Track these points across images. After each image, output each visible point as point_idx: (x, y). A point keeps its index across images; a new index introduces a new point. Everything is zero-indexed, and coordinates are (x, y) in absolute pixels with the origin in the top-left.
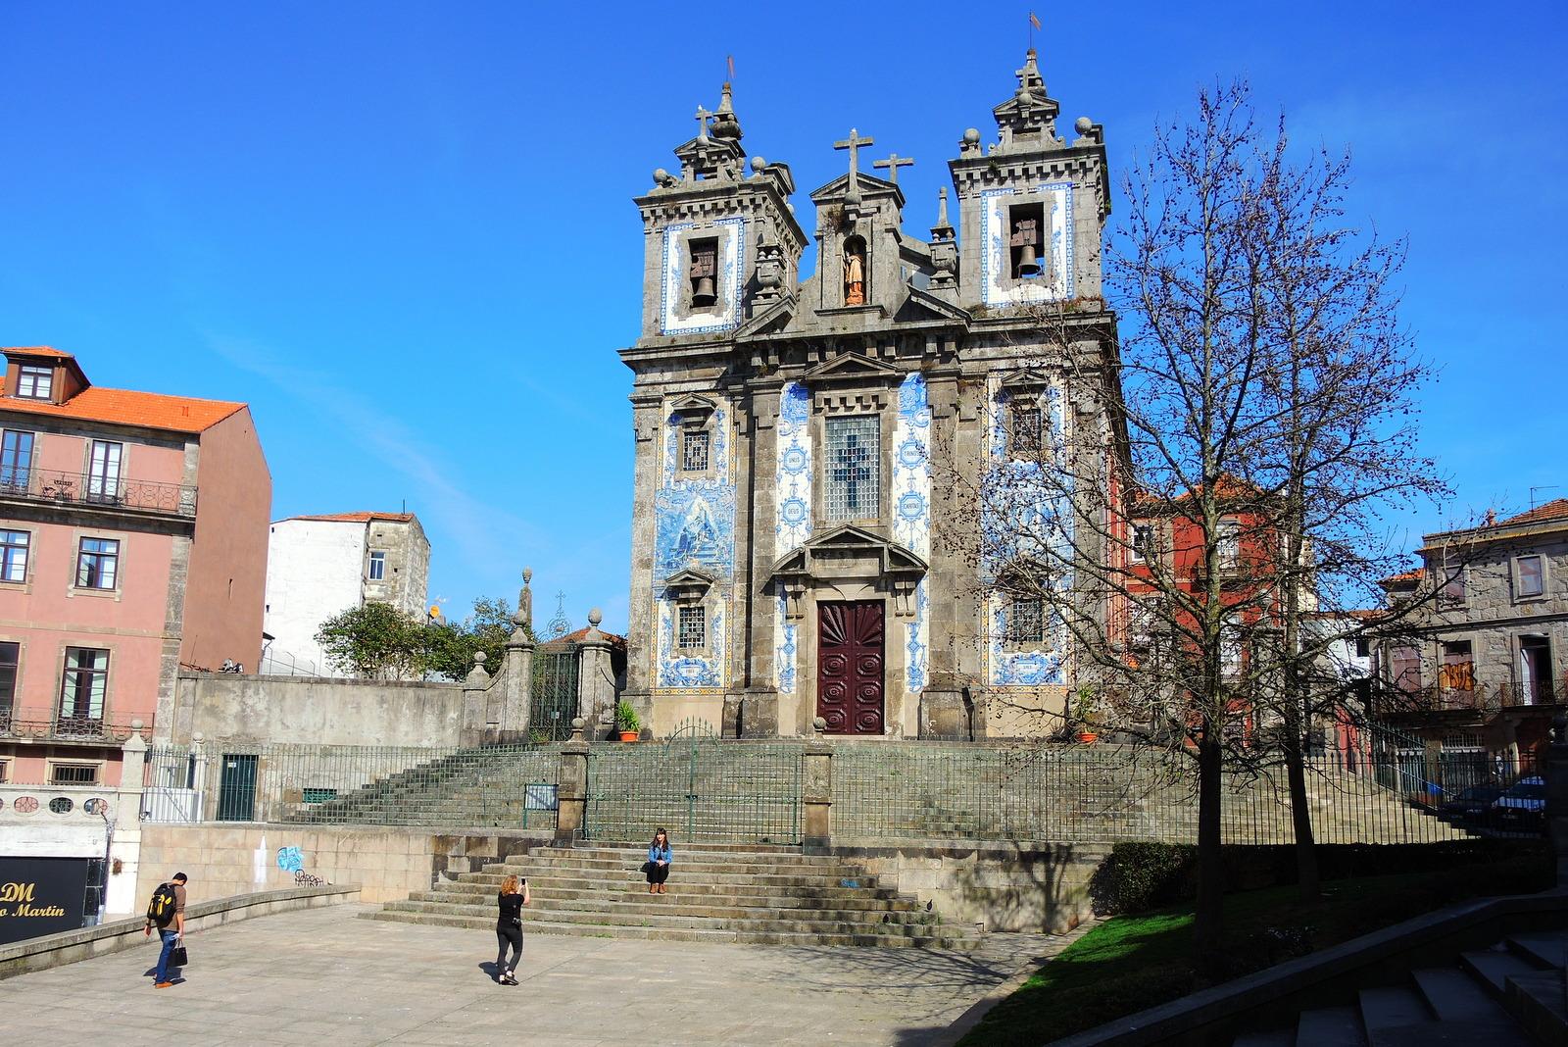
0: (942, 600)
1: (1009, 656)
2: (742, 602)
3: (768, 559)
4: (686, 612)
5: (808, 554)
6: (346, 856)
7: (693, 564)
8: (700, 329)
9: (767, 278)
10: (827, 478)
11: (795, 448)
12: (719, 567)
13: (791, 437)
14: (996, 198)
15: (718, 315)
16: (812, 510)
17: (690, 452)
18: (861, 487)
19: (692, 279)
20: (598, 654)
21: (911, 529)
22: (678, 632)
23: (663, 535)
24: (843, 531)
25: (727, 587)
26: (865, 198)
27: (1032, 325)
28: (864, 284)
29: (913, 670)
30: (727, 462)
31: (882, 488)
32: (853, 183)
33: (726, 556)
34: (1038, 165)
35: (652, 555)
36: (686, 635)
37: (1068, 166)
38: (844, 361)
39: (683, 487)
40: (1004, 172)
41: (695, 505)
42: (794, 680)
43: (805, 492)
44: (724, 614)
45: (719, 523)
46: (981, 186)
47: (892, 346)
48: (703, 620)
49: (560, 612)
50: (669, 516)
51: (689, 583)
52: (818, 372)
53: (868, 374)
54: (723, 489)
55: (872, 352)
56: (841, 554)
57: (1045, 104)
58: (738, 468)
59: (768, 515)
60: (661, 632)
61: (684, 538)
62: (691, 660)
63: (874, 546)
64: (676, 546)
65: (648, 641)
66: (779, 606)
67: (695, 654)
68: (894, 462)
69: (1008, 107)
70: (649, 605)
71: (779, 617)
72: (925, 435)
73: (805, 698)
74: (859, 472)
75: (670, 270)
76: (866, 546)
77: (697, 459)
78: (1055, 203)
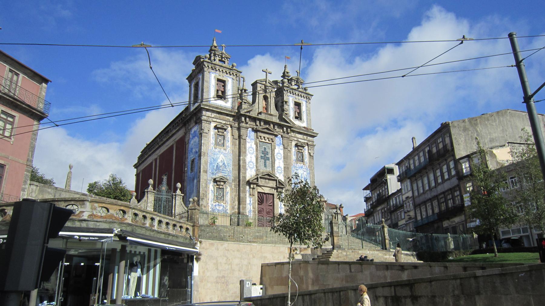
3: (245, 177)
12: (228, 177)
13: (250, 144)
15: (226, 103)
17: (218, 140)
20: (181, 198)
22: (216, 195)
23: (211, 164)
25: (230, 183)
26: (270, 87)
32: (267, 81)
33: (230, 174)
39: (217, 150)
40: (294, 93)
42: (252, 213)
43: (254, 160)
51: (222, 180)
52: (259, 128)
55: (272, 125)
56: (266, 179)
59: (244, 164)
60: (210, 194)
61: (217, 166)
62: (219, 204)
64: (215, 168)
65: (206, 197)
68: (276, 157)
70: (207, 185)
71: (248, 194)
72: (282, 152)
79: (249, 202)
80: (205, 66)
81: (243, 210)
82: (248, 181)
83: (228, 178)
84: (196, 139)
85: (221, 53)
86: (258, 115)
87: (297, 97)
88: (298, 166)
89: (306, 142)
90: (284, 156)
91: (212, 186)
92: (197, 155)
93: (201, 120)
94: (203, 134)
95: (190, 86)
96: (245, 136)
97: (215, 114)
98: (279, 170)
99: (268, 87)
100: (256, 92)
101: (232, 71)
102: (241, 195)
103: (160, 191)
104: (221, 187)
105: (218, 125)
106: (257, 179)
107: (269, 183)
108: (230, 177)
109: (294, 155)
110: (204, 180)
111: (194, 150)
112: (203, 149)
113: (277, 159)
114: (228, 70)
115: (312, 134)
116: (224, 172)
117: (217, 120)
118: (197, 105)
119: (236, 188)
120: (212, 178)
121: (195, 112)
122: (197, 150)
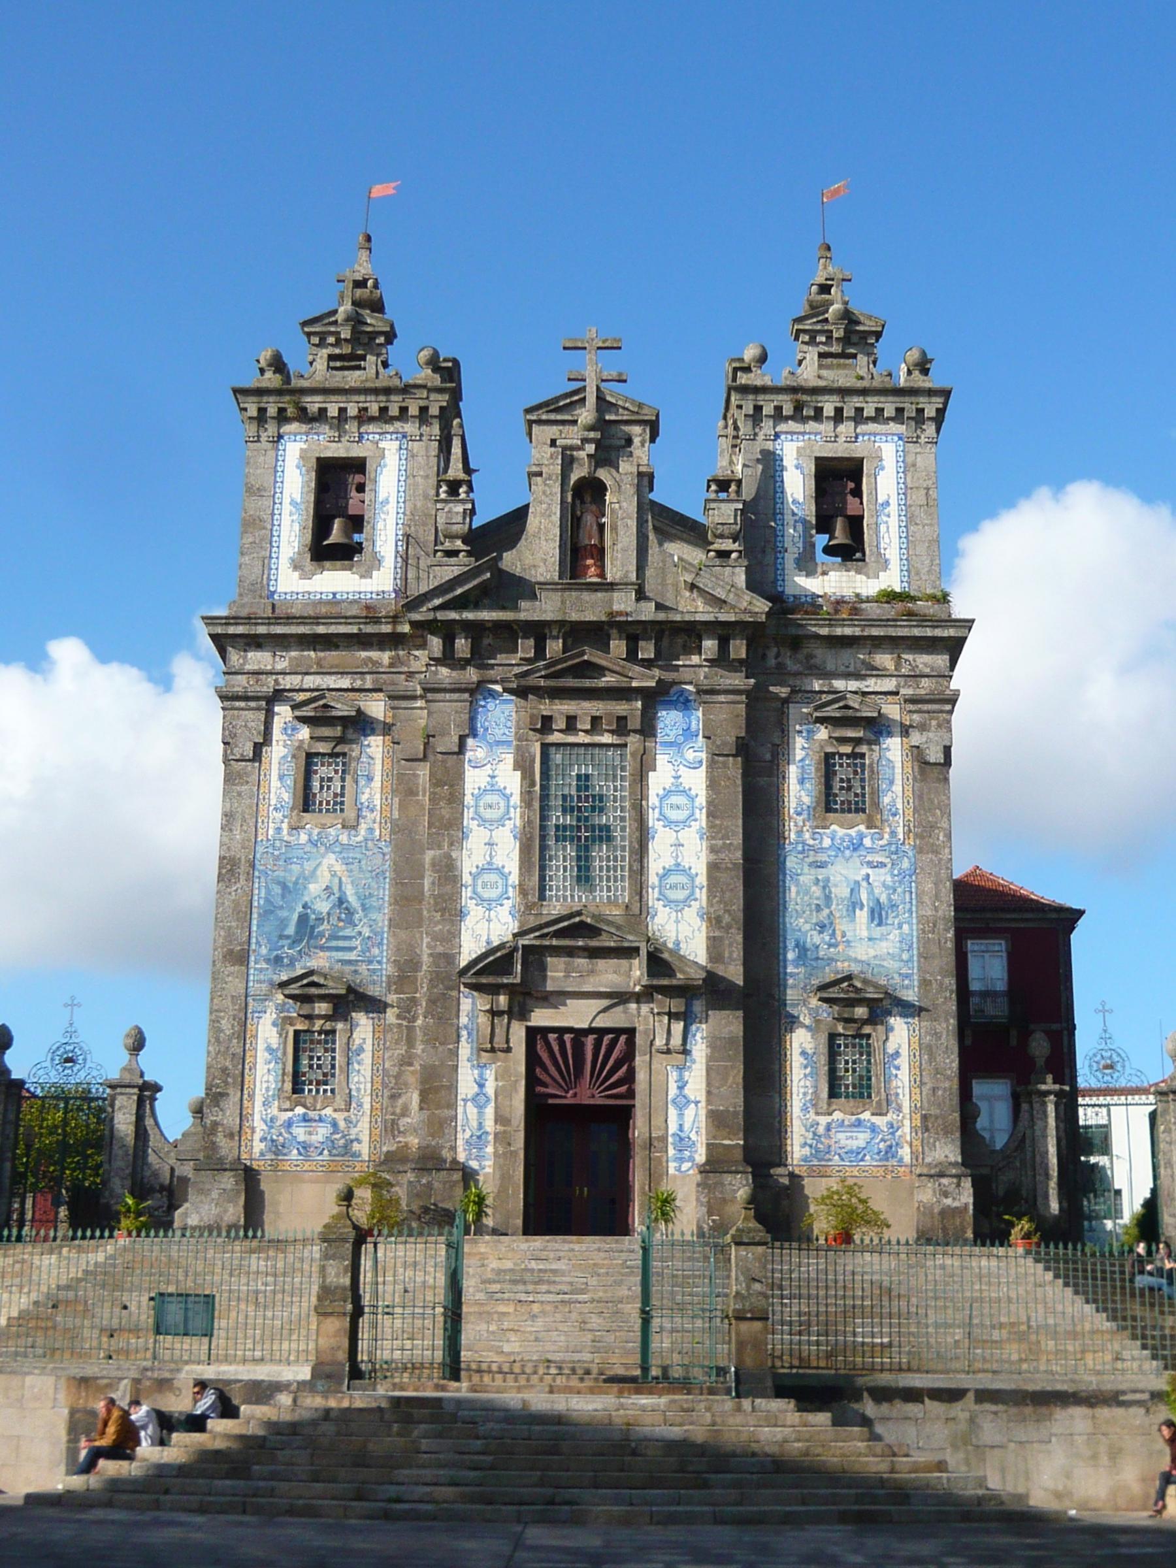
0: (725, 1033)
1: (823, 1120)
2: (400, 1025)
3: (450, 958)
7: (319, 961)
8: (334, 594)
9: (455, 527)
10: (543, 838)
11: (493, 788)
12: (363, 968)
13: (488, 770)
14: (795, 445)
15: (367, 575)
16: (520, 885)
18: (600, 853)
21: (677, 922)
22: (289, 1068)
24: (577, 919)
27: (857, 632)
28: (599, 553)
29: (683, 1142)
30: (377, 802)
34: (858, 405)
36: (304, 1074)
37: (900, 411)
39: (303, 838)
41: (324, 867)
42: (490, 1149)
43: (509, 856)
44: (369, 1042)
45: (363, 899)
47: (648, 639)
48: (334, 1050)
49: (71, 1032)
50: (279, 883)
51: (314, 991)
54: (370, 844)
56: (570, 952)
61: (303, 919)
62: (312, 1114)
63: (626, 944)
64: (291, 930)
68: (652, 818)
72: (697, 781)
73: (505, 1177)
74: (593, 831)
75: (286, 501)
77: (326, 796)
78: (881, 460)
79: (476, 1089)
81: (433, 1136)
87: (826, 427)
88: (827, 842)
89: (889, 685)
90: (710, 803)
91: (274, 1024)
96: (456, 739)
101: (393, 398)
104: (318, 1024)
108: (376, 966)
109: (801, 781)
110: (228, 1002)
113: (658, 825)
114: (373, 398)
115: (929, 632)
116: (346, 944)
117: (308, 678)
119: (414, 1019)
120: (271, 983)
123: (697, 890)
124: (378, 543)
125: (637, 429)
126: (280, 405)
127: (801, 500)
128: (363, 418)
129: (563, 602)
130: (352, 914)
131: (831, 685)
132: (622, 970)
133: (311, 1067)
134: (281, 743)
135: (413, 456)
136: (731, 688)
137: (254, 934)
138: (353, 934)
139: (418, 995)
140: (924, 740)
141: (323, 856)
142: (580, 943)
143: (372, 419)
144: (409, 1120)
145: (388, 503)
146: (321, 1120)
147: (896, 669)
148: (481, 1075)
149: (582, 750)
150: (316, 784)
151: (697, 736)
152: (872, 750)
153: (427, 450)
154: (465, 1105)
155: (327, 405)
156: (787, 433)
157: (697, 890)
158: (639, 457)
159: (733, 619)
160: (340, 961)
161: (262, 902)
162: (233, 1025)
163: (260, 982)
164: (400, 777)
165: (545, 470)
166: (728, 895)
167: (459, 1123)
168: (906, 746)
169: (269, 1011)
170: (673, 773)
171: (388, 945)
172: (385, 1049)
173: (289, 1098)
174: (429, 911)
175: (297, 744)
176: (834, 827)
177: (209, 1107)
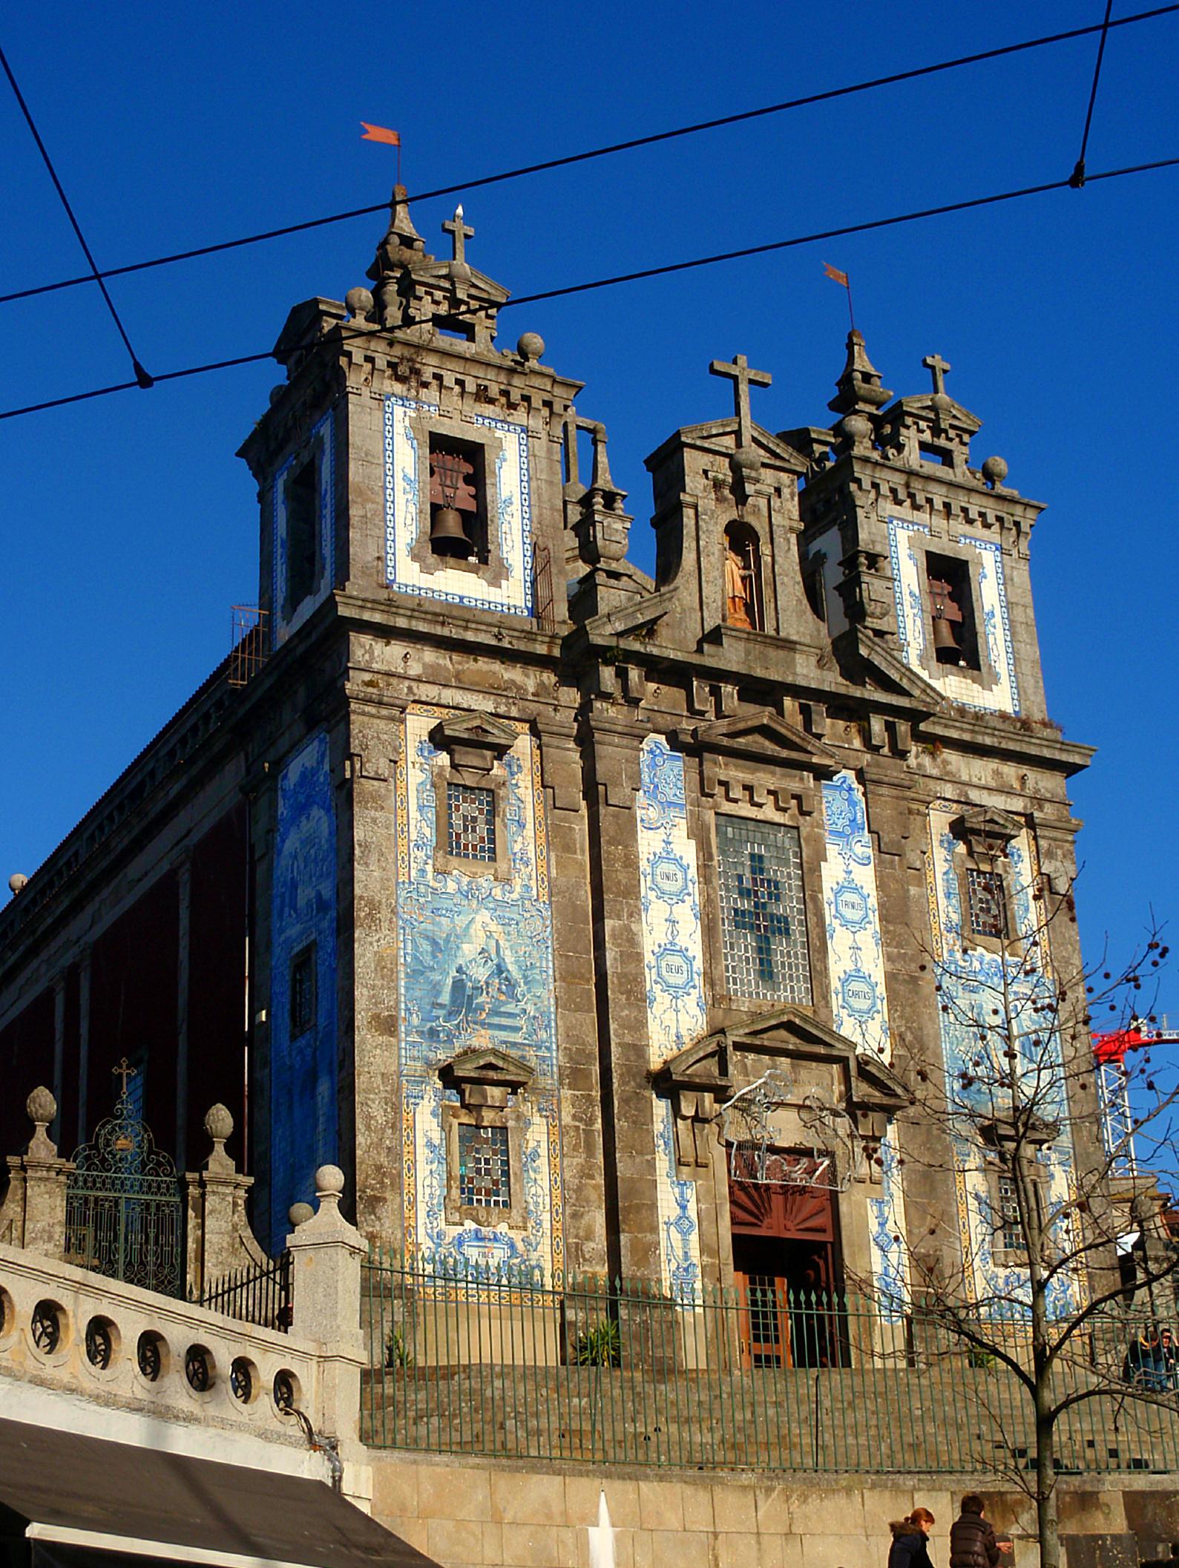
2: (577, 1128)
3: (639, 1051)
4: (471, 1135)
5: (730, 1049)
6: (779, 1541)
7: (482, 1039)
8: (461, 598)
11: (667, 856)
12: (530, 1053)
15: (495, 582)
18: (779, 946)
19: (433, 505)
20: (235, 1204)
22: (457, 1171)
23: (416, 973)
24: (785, 1018)
26: (764, 465)
30: (532, 855)
31: (815, 956)
34: (963, 504)
35: (397, 1007)
38: (755, 723)
39: (452, 887)
40: (920, 499)
41: (477, 926)
44: (544, 1145)
45: (526, 969)
46: (888, 507)
48: (506, 1152)
50: (427, 938)
51: (492, 1075)
53: (795, 755)
57: (964, 419)
58: (554, 872)
59: (631, 968)
60: (423, 1170)
61: (458, 986)
62: (485, 1231)
63: (835, 1053)
64: (445, 998)
65: (397, 1184)
66: (661, 1142)
67: (494, 1220)
68: (828, 913)
69: (919, 405)
70: (397, 1109)
71: (663, 1163)
72: (866, 877)
75: (399, 475)
76: (823, 1052)
79: (678, 1211)
80: (350, 363)
82: (664, 1074)
83: (533, 1063)
84: (319, 822)
85: (444, 271)
86: (700, 650)
88: (976, 965)
89: (1018, 805)
91: (434, 1114)
92: (325, 924)
93: (345, 701)
94: (363, 788)
95: (261, 497)
96: (628, 790)
97: (429, 655)
98: (856, 994)
99: (751, 467)
100: (679, 506)
101: (517, 381)
102: (622, 1169)
103: (104, 1160)
105: (451, 722)
106: (721, 1054)
107: (796, 1081)
109: (948, 896)
111: (305, 895)
112: (366, 879)
113: (836, 923)
114: (491, 374)
118: (308, 607)
119: (591, 1122)
120: (429, 1064)
121: (300, 650)
122: (327, 891)
123: (879, 1002)
124: (505, 548)
125: (785, 477)
126: (389, 358)
127: (917, 594)
128: (482, 395)
129: (748, 653)
130: (514, 987)
131: (966, 795)
132: (825, 1085)
133: (478, 1171)
134: (417, 766)
135: (535, 456)
136: (896, 781)
137: (403, 999)
138: (518, 1012)
139: (593, 1093)
140: (1052, 869)
141: (476, 912)
142: (791, 1047)
143: (491, 401)
144: (594, 1246)
145: (511, 503)
146: (496, 1239)
147: (1022, 790)
148: (682, 1194)
149: (751, 825)
150: (457, 821)
151: (863, 829)
152: (1006, 872)
153: (549, 451)
154: (668, 1231)
155: (443, 372)
156: (898, 519)
157: (879, 1002)
158: (789, 511)
159: (908, 706)
160: (505, 1042)
161: (409, 959)
162: (385, 1111)
163: (414, 1059)
164: (556, 827)
165: (700, 503)
166: (908, 1009)
167: (662, 1253)
168: (1035, 874)
169: (426, 1100)
170: (845, 867)
171: (557, 1030)
172: (563, 1155)
173: (458, 1209)
174: (612, 990)
175: (436, 770)
176: (980, 950)
177: (363, 1214)
